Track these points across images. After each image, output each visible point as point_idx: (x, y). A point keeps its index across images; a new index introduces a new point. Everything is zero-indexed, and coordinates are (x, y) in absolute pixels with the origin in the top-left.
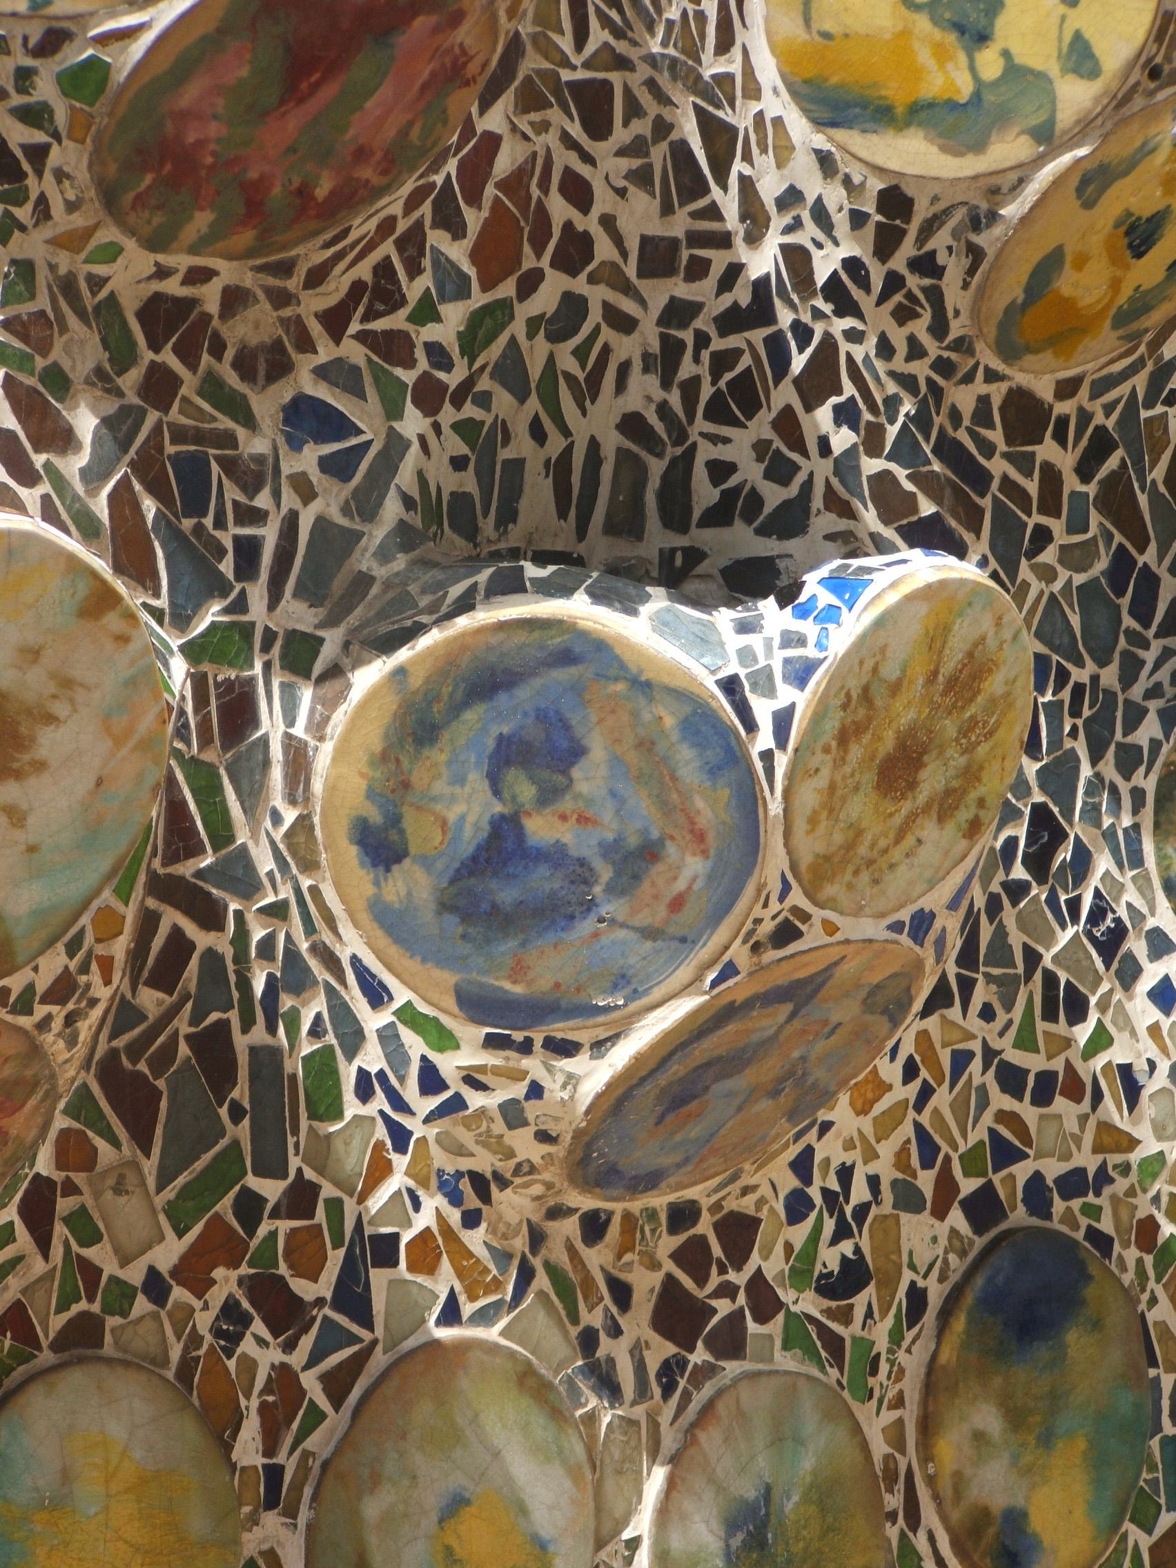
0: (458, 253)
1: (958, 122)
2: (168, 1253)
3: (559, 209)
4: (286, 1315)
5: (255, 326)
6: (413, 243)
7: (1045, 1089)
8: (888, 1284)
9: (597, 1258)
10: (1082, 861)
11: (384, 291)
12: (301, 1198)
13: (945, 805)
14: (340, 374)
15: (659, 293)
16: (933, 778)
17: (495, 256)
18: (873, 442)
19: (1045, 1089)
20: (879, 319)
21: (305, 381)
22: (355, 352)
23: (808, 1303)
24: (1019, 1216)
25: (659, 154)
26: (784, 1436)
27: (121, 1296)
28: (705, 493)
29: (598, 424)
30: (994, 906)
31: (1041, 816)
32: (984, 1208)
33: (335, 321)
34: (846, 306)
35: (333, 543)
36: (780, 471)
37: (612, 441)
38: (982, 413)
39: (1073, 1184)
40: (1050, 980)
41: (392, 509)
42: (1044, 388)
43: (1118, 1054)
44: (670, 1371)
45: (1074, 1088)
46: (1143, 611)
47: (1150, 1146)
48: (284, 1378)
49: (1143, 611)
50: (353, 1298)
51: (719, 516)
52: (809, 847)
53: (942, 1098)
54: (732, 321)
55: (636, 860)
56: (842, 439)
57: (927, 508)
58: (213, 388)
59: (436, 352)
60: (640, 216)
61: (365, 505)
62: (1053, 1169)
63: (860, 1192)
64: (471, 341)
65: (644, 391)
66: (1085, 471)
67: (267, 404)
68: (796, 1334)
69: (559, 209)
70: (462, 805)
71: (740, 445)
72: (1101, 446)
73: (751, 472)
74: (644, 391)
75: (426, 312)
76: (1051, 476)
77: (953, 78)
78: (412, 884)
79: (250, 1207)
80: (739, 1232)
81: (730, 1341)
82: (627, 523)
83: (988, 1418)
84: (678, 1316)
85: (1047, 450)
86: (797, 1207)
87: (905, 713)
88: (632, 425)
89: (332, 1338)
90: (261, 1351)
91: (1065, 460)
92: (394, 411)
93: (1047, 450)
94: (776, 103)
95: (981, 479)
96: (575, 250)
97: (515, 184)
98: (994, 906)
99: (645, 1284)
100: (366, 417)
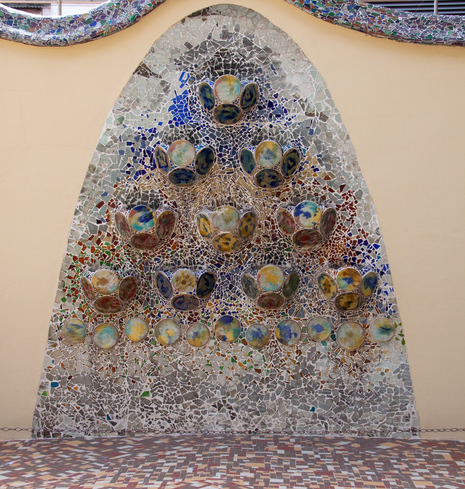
0: (170, 248)
1: (208, 237)
2: (143, 312)
3: (179, 244)
4: (154, 316)
5: (152, 254)
6: (165, 248)
7: (231, 305)
8: (212, 318)
9: (182, 315)
10: (236, 288)
11: (163, 251)
12: (155, 309)
13: (190, 285)
14: (160, 256)
15: (190, 249)
16: (187, 283)
17: (173, 248)
18: (211, 258)
19: (231, 305)
20: (210, 250)
21: (156, 257)
22: (160, 255)
23: (204, 319)
24: (227, 314)
25: (189, 240)
26: (199, 328)
27: (140, 314)
28: (196, 262)
29: (187, 257)
30: (225, 292)
31: (230, 285)
32: (223, 314)
33: (159, 253)
34: (207, 249)
35: (157, 267)
36: (202, 261)
37: (188, 259)
38: (223, 255)
39: (233, 313)
40: (231, 297)
41: (162, 265)
42: (229, 254)
43: (240, 303)
44: (189, 323)
45: (234, 305)
46: (242, 269)
47: (243, 310)
48: (153, 320)
49: (242, 269)
50: (159, 315)
51: (198, 264)
52: (177, 288)
53: (219, 305)
54: (196, 250)
55: (168, 288)
56: (207, 258)
57: (217, 262)
58: (149, 258)
59: (168, 255)
60: (187, 244)
61: (161, 265)
62: (231, 311)
63: (209, 311)
64: (172, 253)
65: (190, 256)
66: (235, 259)
67: (153, 259)
68: (202, 321)
69: (179, 244)
70: (160, 284)
71: (199, 259)
72: (237, 257)
73: (200, 261)
74: (190, 256)
75: (167, 252)
76: (232, 260)
77: (207, 234)
78: (160, 289)
79: (150, 309)
80: (196, 314)
81: (195, 321)
82: (191, 264)
83: (222, 329)
84: (190, 319)
85: (231, 258)
86: (203, 312)
87: (182, 279)
88: (189, 258)
89: (157, 318)
90: (151, 318)
91: (233, 259)
92: (164, 258)
93: (231, 258)
94: (200, 236)
95: (224, 260)
96: (181, 247)
97: (176, 243)
98: (225, 292)
99: (187, 317)
100: (162, 259)
